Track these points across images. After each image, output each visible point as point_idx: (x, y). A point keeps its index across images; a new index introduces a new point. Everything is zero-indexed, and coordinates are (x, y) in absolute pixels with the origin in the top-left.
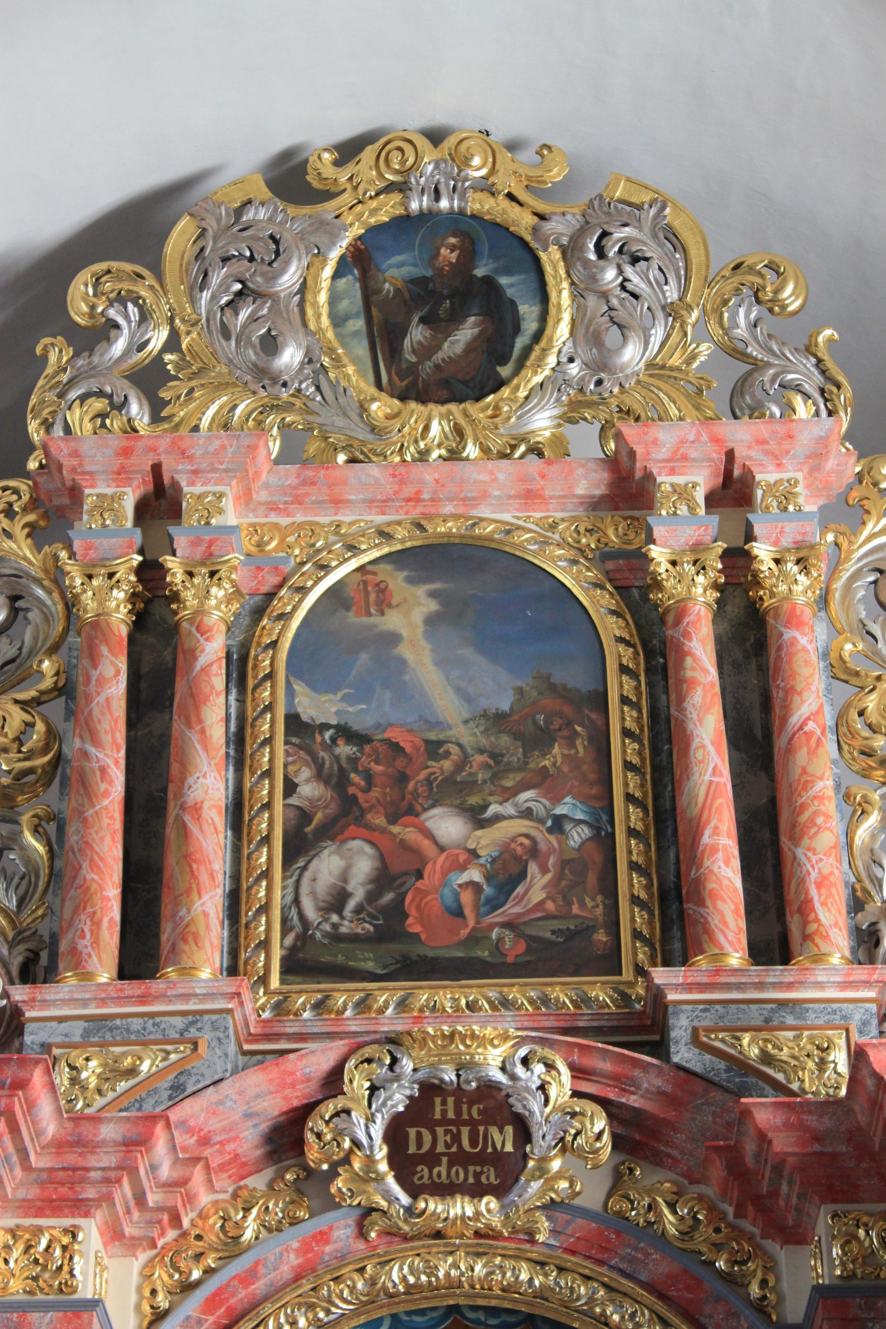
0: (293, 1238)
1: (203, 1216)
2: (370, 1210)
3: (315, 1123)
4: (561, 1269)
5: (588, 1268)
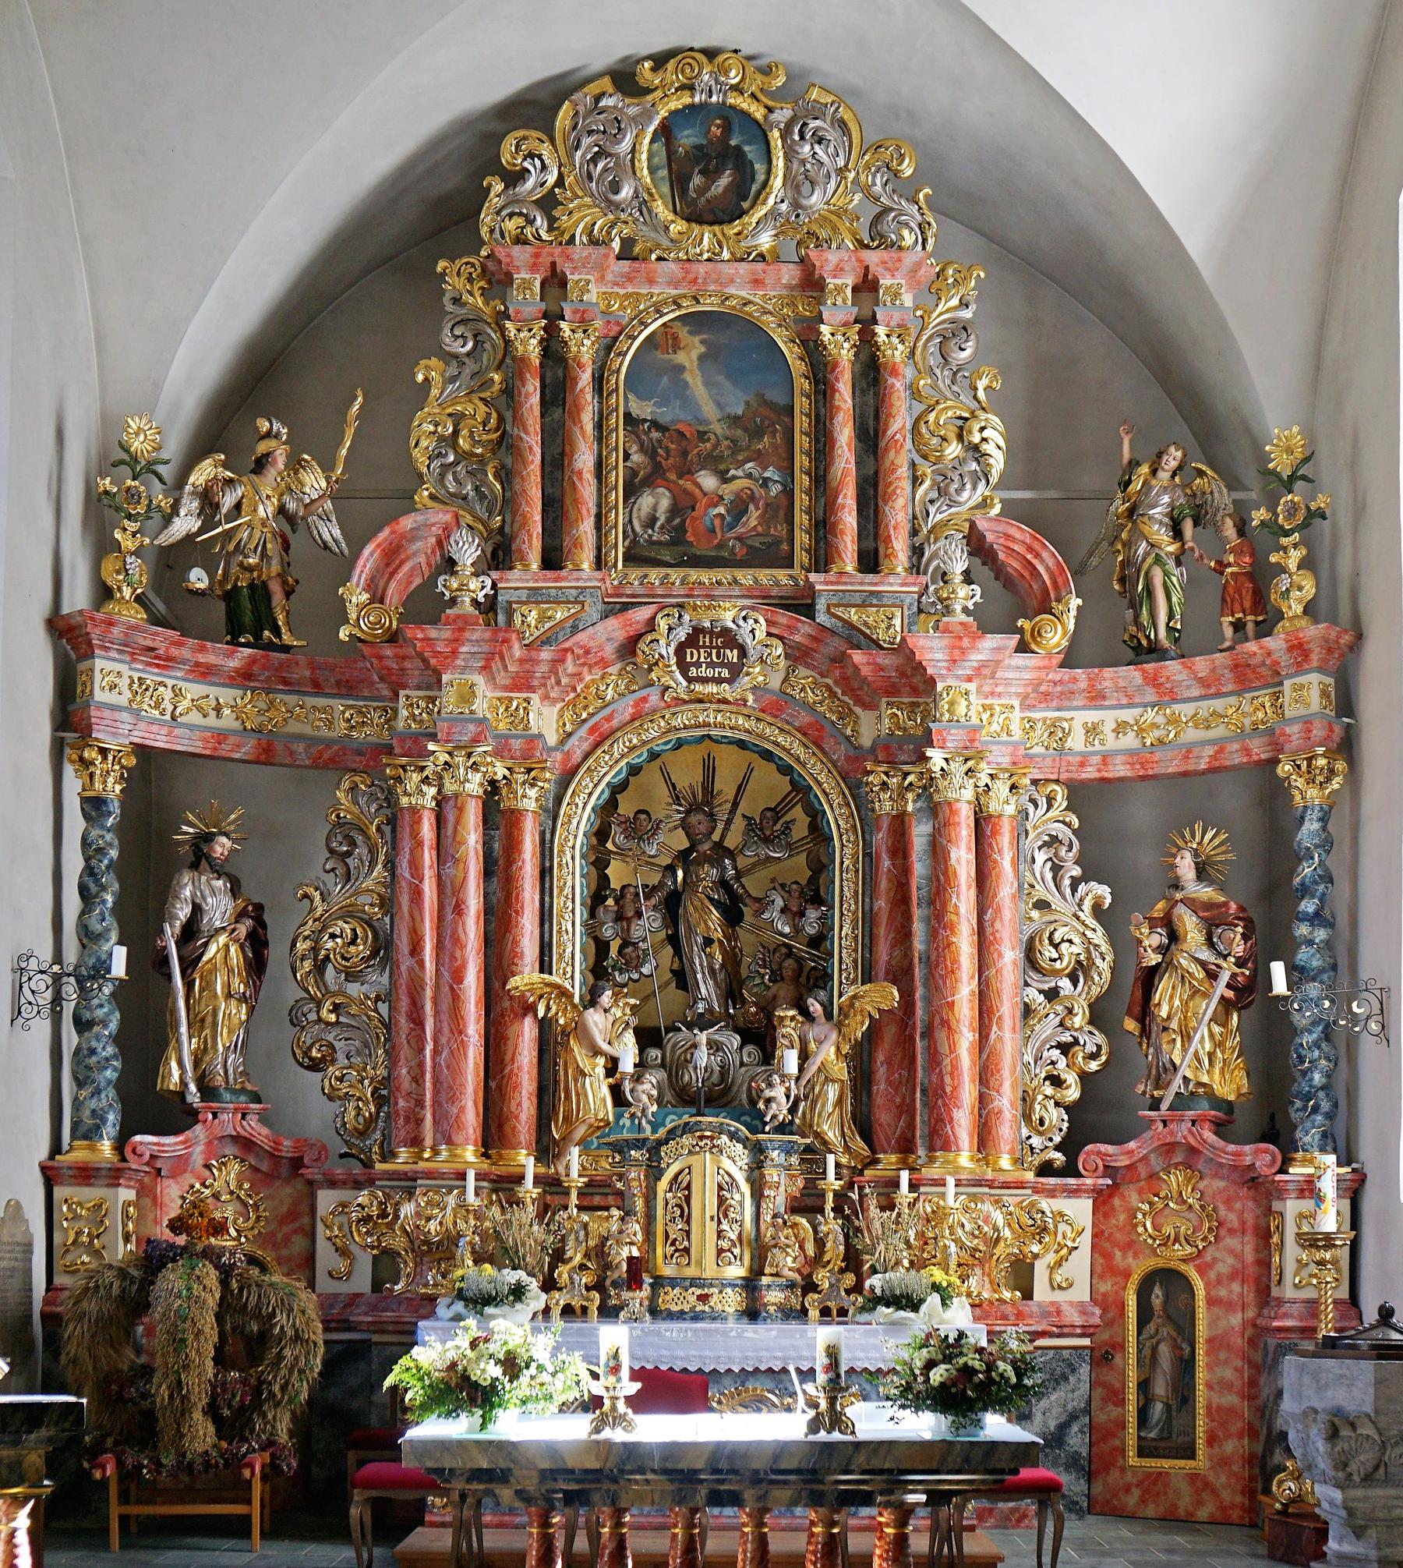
0: (631, 699)
1: (587, 687)
2: (668, 687)
3: (641, 645)
4: (758, 719)
5: (770, 719)
